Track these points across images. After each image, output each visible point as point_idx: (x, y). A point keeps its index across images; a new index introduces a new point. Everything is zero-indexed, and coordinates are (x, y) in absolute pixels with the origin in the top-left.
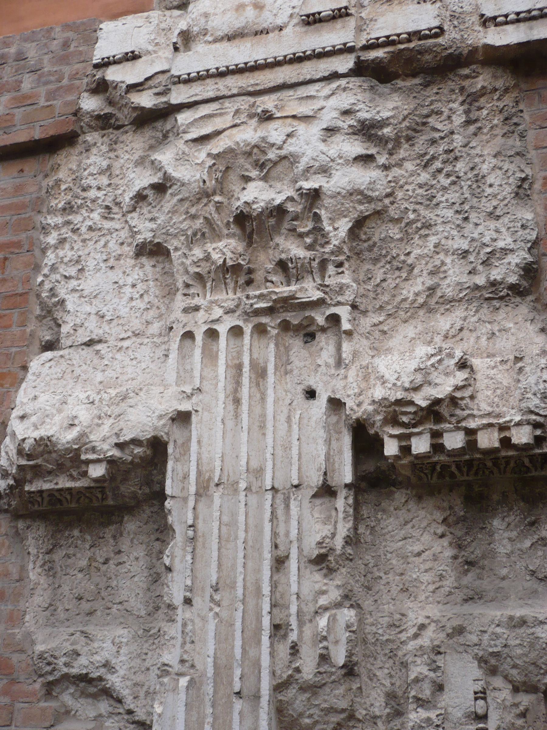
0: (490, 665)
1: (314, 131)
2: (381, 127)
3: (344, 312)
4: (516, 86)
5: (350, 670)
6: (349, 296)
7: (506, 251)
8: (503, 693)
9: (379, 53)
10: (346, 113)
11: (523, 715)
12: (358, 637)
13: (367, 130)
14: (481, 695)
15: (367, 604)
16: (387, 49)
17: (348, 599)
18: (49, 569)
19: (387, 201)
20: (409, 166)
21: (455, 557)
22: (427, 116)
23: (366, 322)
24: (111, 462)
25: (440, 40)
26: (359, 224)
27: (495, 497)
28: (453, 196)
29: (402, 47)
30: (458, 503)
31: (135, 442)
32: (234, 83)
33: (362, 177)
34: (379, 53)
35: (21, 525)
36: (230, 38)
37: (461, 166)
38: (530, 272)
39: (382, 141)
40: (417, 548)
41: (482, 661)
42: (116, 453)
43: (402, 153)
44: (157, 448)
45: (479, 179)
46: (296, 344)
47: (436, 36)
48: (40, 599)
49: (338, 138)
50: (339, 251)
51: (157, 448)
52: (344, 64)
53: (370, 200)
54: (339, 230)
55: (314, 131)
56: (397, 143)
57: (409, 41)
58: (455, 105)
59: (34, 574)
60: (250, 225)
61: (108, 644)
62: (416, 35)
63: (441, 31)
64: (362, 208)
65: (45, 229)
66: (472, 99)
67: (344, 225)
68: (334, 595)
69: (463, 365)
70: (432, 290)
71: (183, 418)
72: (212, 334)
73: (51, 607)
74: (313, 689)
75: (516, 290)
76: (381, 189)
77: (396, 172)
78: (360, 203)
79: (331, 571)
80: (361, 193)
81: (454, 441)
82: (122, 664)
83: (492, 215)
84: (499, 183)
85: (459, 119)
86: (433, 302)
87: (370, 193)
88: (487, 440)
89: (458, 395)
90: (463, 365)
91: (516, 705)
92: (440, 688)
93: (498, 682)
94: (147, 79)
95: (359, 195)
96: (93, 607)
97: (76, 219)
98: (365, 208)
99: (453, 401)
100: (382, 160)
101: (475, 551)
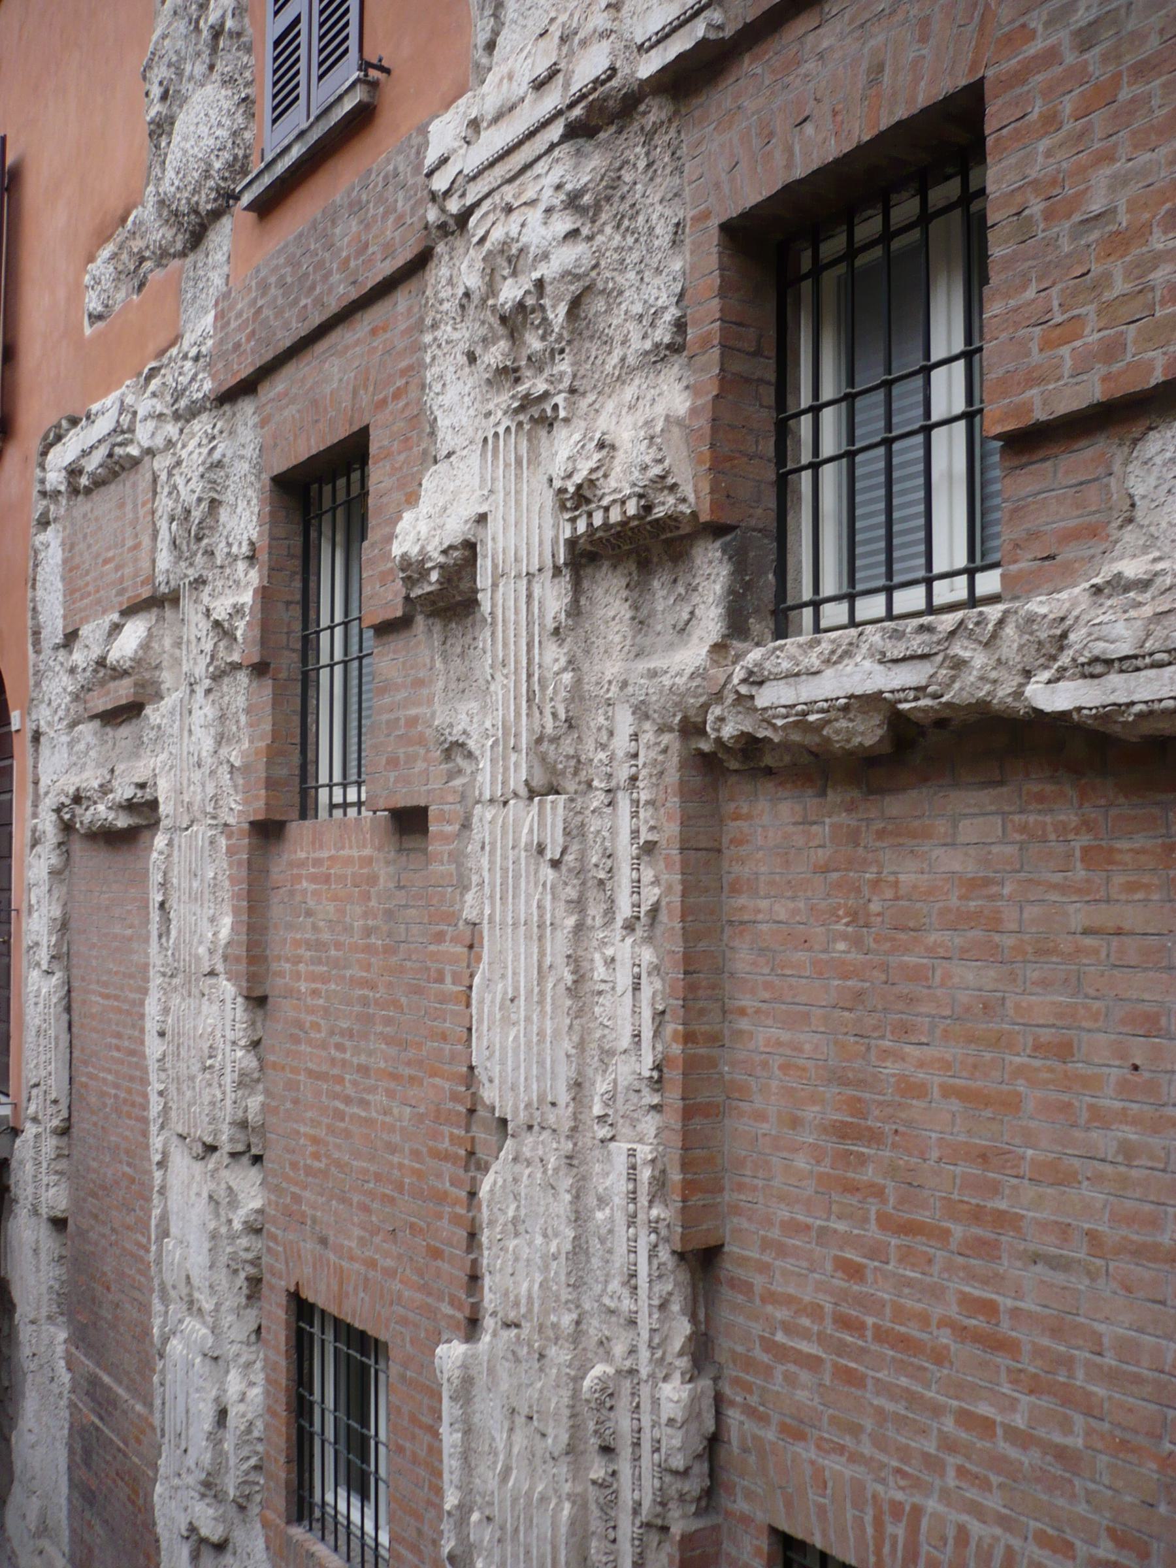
0: (641, 712)
1: (535, 216)
2: (582, 196)
3: (559, 399)
4: (676, 113)
5: (570, 724)
6: (566, 384)
7: (665, 309)
8: (648, 737)
9: (577, 111)
10: (559, 187)
11: (665, 751)
12: (576, 693)
13: (573, 202)
14: (635, 737)
15: (586, 667)
16: (583, 104)
17: (572, 664)
18: (445, 659)
19: (593, 274)
20: (608, 230)
21: (633, 618)
22: (620, 169)
23: (583, 404)
24: (442, 567)
25: (614, 83)
26: (575, 304)
27: (655, 560)
28: (635, 256)
29: (591, 98)
30: (633, 567)
31: (451, 547)
32: (501, 171)
33: (566, 257)
34: (577, 111)
35: (430, 621)
36: (496, 119)
37: (641, 219)
38: (680, 326)
39: (581, 210)
40: (612, 614)
41: (636, 710)
42: (442, 559)
43: (604, 217)
44: (470, 547)
45: (651, 229)
46: (543, 433)
47: (609, 78)
48: (440, 684)
49: (555, 216)
50: (560, 338)
51: (470, 547)
52: (556, 131)
53: (578, 277)
54: (558, 314)
55: (535, 216)
56: (597, 207)
57: (594, 89)
58: (638, 149)
59: (439, 664)
60: (515, 321)
61: (464, 716)
62: (598, 82)
63: (613, 70)
64: (573, 288)
65: (425, 348)
66: (649, 137)
67: (563, 309)
68: (563, 661)
69: (601, 445)
70: (623, 359)
71: (482, 519)
72: (496, 434)
73: (445, 690)
74: (555, 740)
75: (675, 348)
76: (587, 263)
77: (600, 238)
78: (571, 283)
79: (561, 642)
80: (569, 273)
81: (598, 520)
82: (475, 730)
83: (658, 271)
84: (663, 232)
85: (642, 164)
86: (625, 374)
87: (578, 271)
88: (615, 516)
89: (594, 477)
90: (601, 445)
91: (659, 744)
92: (611, 734)
93: (647, 725)
94: (453, 182)
95: (568, 275)
96: (464, 685)
97: (439, 333)
98: (575, 288)
99: (592, 483)
100: (585, 231)
101: (644, 612)
